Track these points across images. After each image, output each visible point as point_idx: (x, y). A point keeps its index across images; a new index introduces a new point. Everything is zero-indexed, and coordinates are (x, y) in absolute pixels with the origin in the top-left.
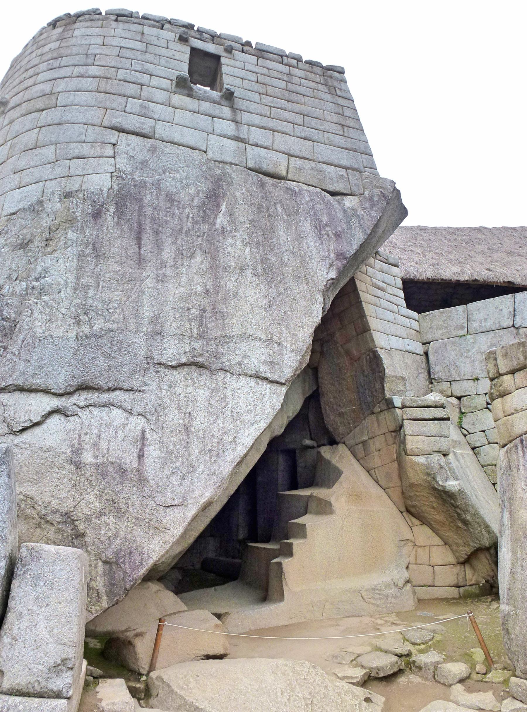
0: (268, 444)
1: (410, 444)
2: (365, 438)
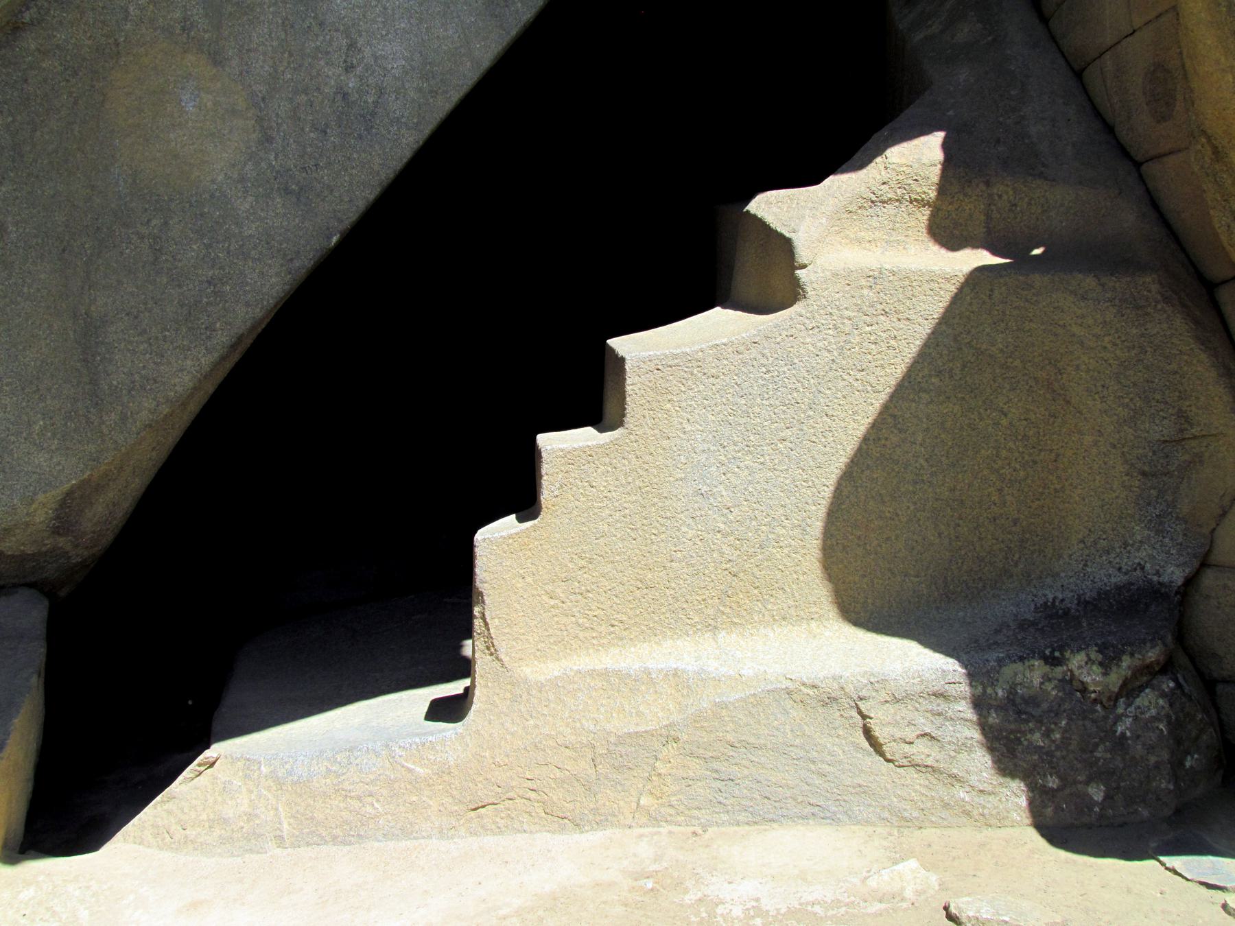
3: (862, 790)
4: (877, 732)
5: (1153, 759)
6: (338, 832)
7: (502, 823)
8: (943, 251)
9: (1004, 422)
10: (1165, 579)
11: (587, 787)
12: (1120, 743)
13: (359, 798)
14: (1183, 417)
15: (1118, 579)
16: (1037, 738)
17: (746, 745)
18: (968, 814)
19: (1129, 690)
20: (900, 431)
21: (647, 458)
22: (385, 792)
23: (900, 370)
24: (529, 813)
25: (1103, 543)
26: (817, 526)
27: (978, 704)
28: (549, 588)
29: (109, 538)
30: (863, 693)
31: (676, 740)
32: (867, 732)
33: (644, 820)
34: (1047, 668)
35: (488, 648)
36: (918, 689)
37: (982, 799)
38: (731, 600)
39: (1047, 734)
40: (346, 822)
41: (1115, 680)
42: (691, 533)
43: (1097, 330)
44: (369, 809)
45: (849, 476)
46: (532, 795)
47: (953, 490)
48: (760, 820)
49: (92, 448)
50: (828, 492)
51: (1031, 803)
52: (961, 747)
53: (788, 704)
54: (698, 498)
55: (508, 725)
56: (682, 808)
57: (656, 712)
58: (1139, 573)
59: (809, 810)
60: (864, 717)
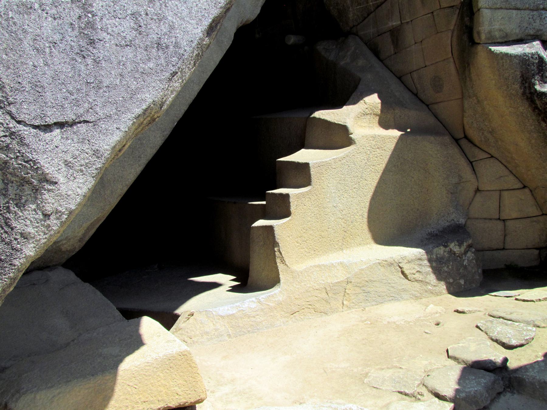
0: (236, 34)
1: (486, 23)
2: (395, 23)
3: (404, 290)
4: (407, 272)
5: (473, 271)
6: (249, 329)
7: (302, 317)
8: (384, 130)
9: (413, 180)
10: (460, 223)
11: (327, 301)
12: (465, 267)
13: (254, 317)
14: (460, 177)
15: (447, 224)
16: (445, 269)
17: (371, 281)
18: (432, 293)
19: (466, 252)
20: (386, 184)
21: (319, 195)
22: (262, 313)
23: (384, 166)
24: (310, 313)
25: (442, 214)
26: (366, 215)
27: (430, 260)
28: (296, 240)
29: (78, 246)
30: (400, 261)
31: (351, 282)
32: (403, 273)
33: (346, 309)
34: (444, 248)
35: (282, 261)
36: (414, 258)
37: (434, 288)
38: (345, 241)
39: (448, 267)
40: (252, 325)
41: (463, 249)
42: (333, 219)
43: (436, 152)
44: (259, 320)
45: (373, 198)
46: (310, 306)
47: (401, 201)
48: (378, 303)
49: (102, 204)
50: (368, 204)
51: (447, 287)
52: (427, 274)
53: (380, 267)
54: (334, 208)
55: (295, 286)
56: (356, 303)
57: (341, 276)
58: (453, 222)
59: (391, 298)
60: (401, 268)
